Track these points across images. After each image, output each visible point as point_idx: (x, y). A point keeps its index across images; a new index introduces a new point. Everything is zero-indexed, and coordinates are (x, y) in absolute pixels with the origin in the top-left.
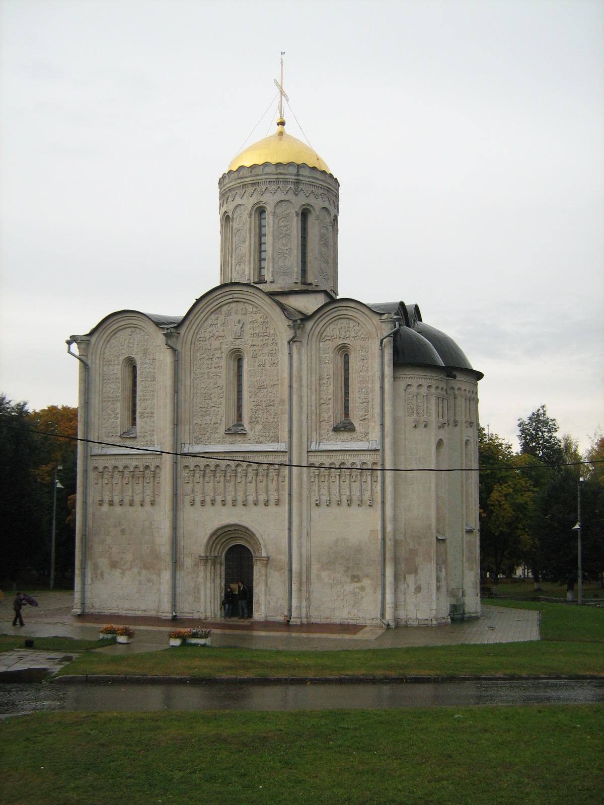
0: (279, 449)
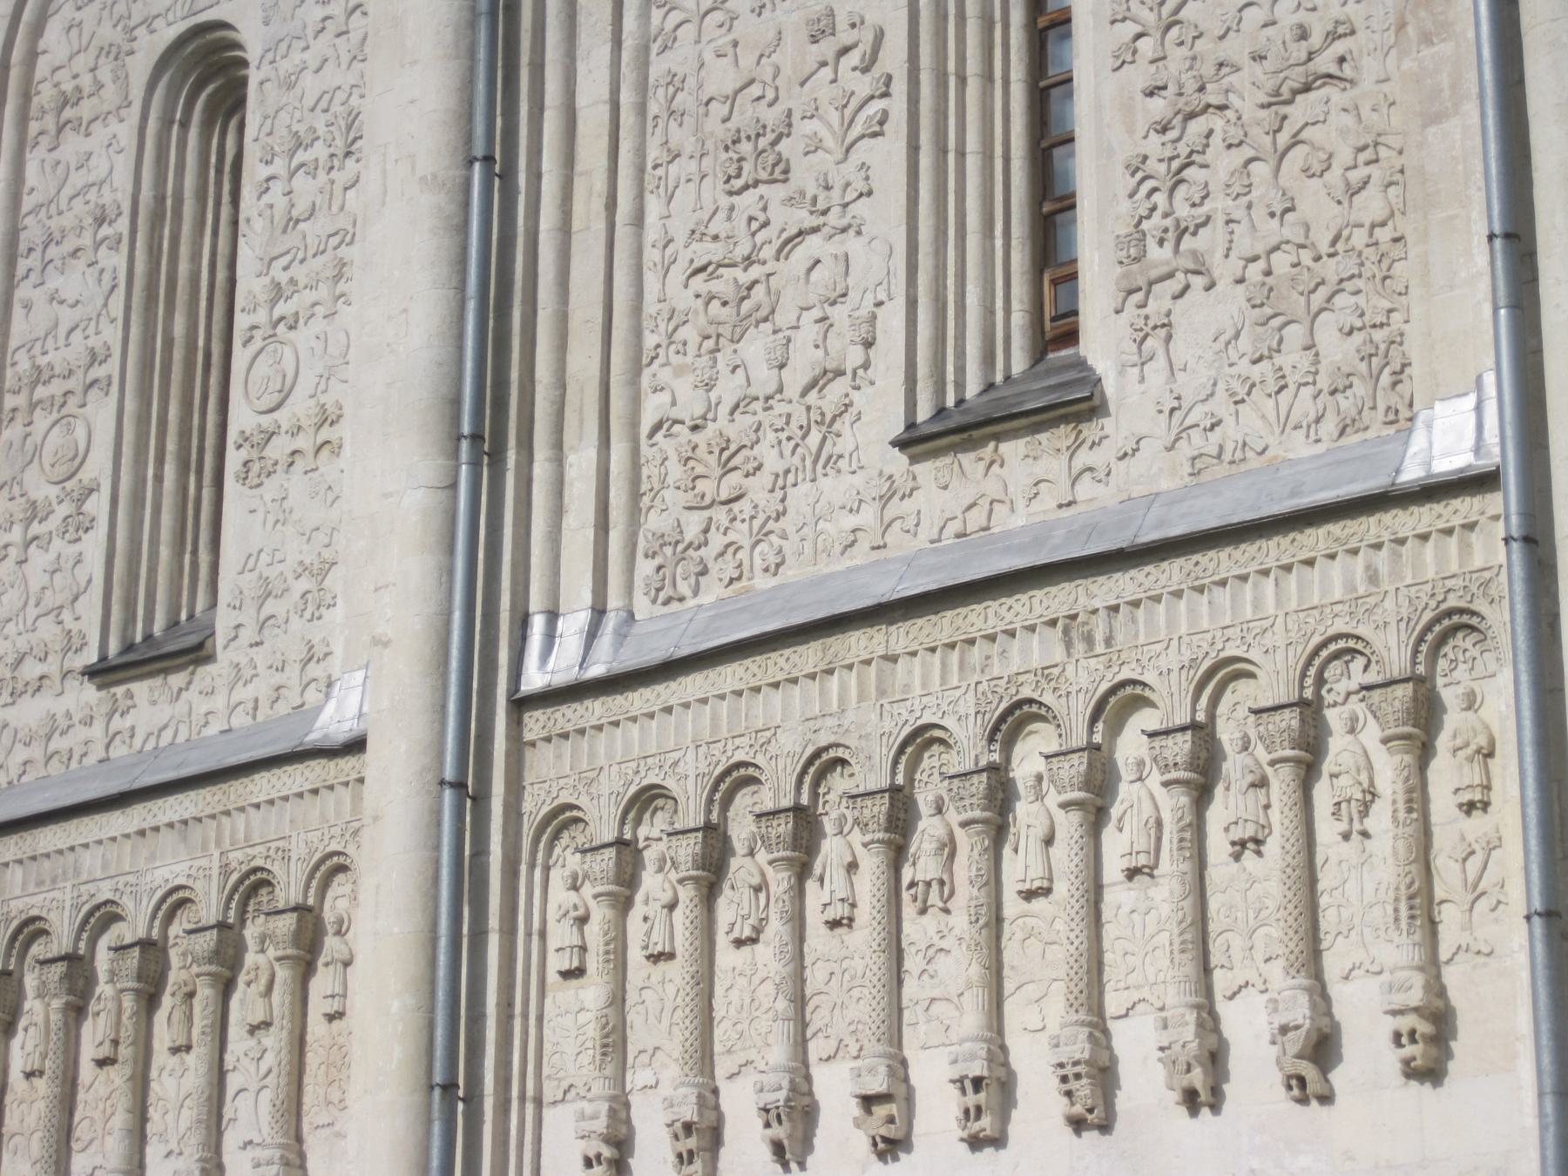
0: (1411, 474)
